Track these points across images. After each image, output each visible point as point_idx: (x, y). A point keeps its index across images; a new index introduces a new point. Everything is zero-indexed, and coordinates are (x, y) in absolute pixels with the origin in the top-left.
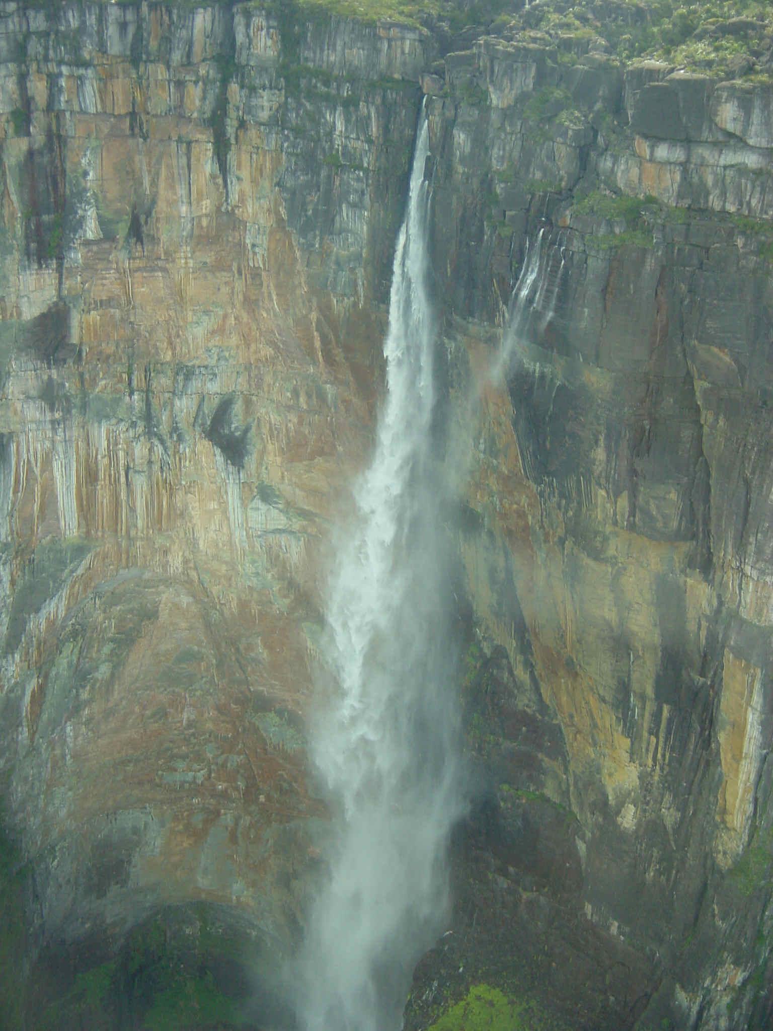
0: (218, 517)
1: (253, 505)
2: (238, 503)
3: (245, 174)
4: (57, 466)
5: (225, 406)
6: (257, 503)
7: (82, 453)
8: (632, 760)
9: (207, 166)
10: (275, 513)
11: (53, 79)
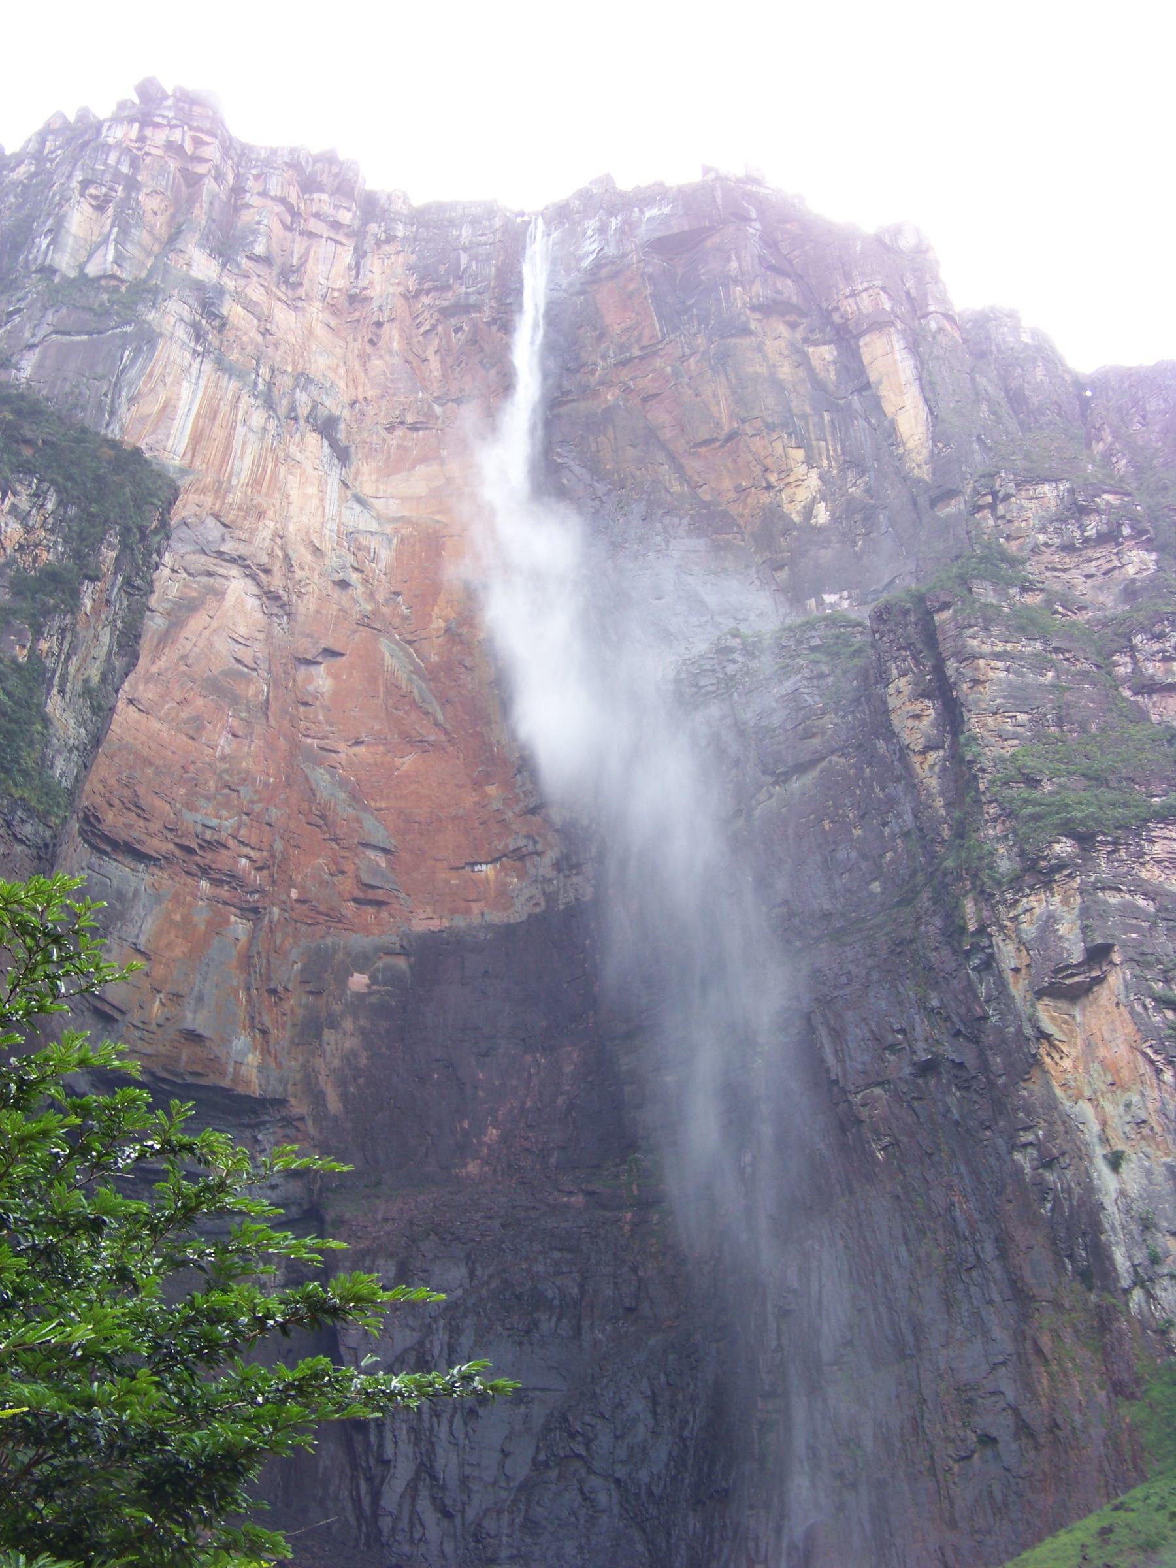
0: (315, 502)
1: (349, 504)
2: (335, 496)
4: (185, 384)
7: (211, 391)
8: (810, 467)
9: (347, 257)
10: (366, 515)
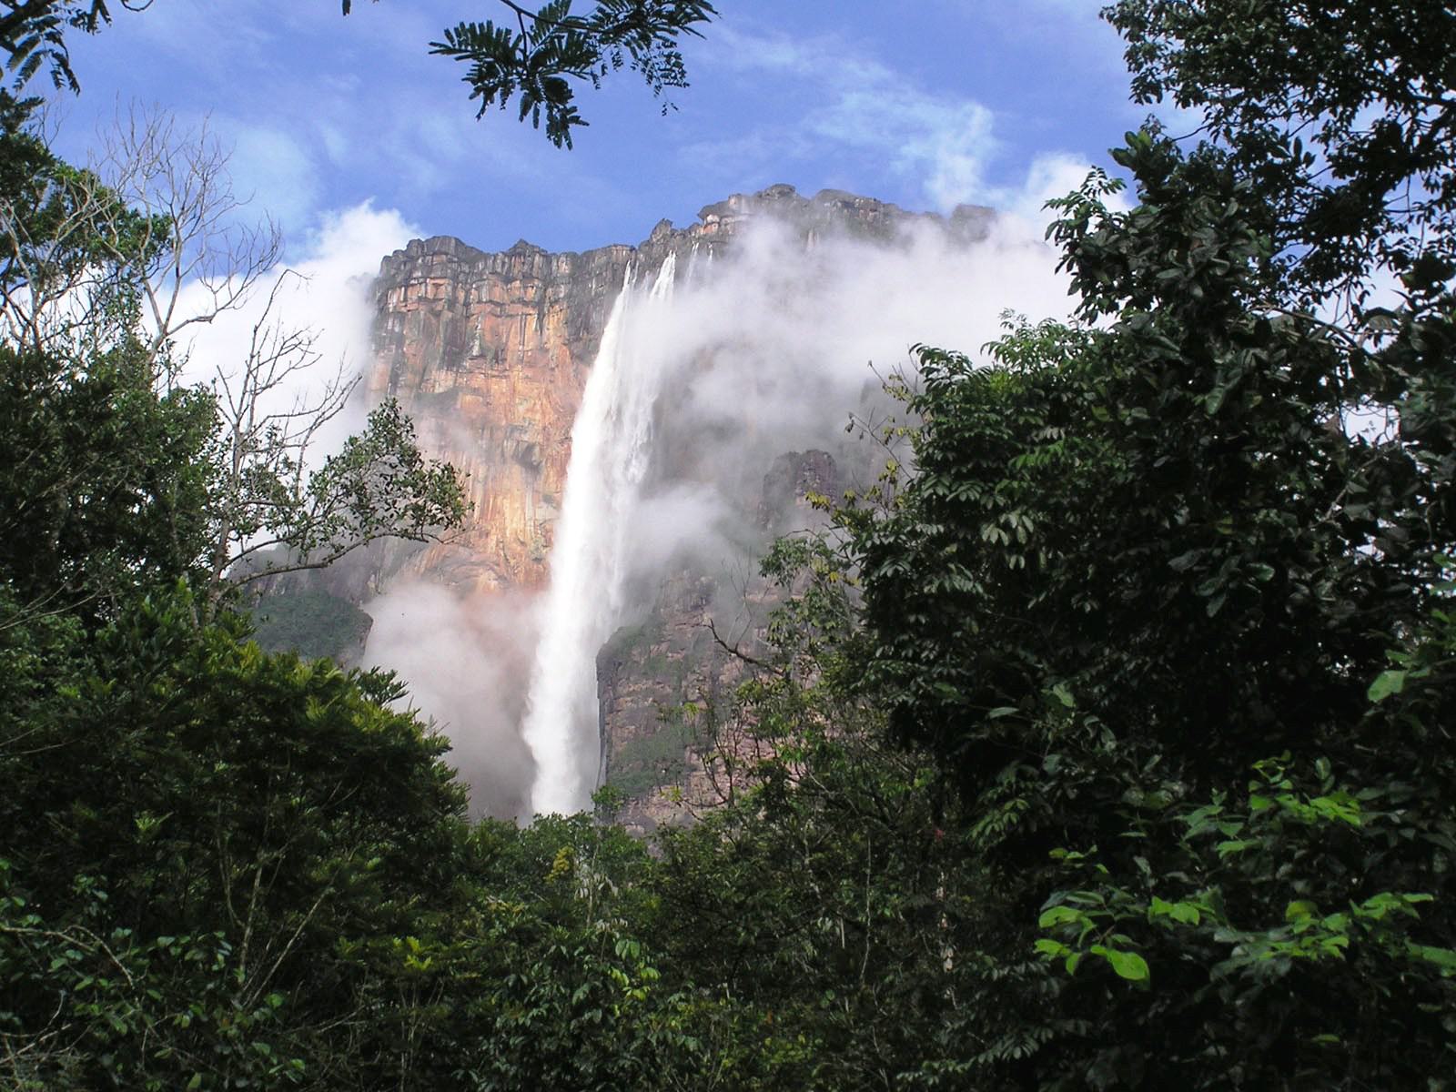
3: (551, 326)
5: (530, 448)
6: (542, 503)
9: (532, 323)
11: (468, 293)
